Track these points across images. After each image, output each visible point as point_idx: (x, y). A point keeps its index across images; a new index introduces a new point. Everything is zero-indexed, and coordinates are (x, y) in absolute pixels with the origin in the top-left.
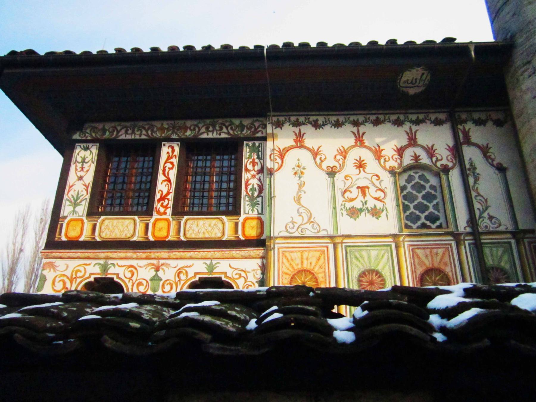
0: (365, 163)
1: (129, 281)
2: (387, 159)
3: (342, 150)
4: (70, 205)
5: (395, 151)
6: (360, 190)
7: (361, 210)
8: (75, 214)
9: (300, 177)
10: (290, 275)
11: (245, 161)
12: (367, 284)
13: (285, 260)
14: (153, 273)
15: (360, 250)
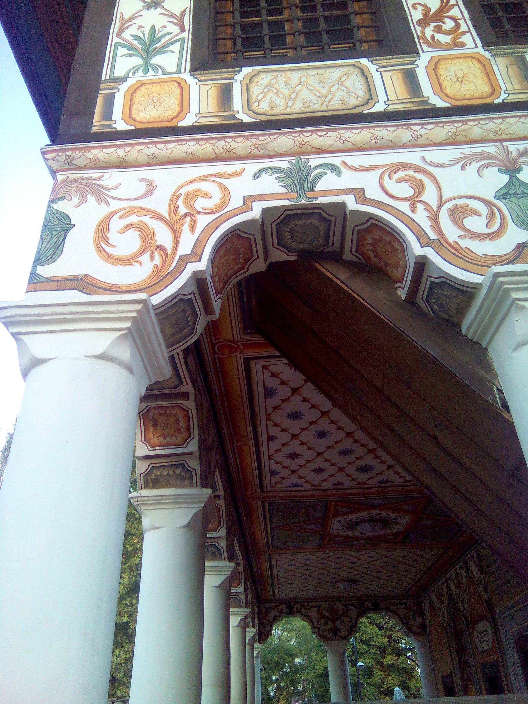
1: (413, 208)
4: (131, 55)
8: (151, 72)
14: (497, 179)
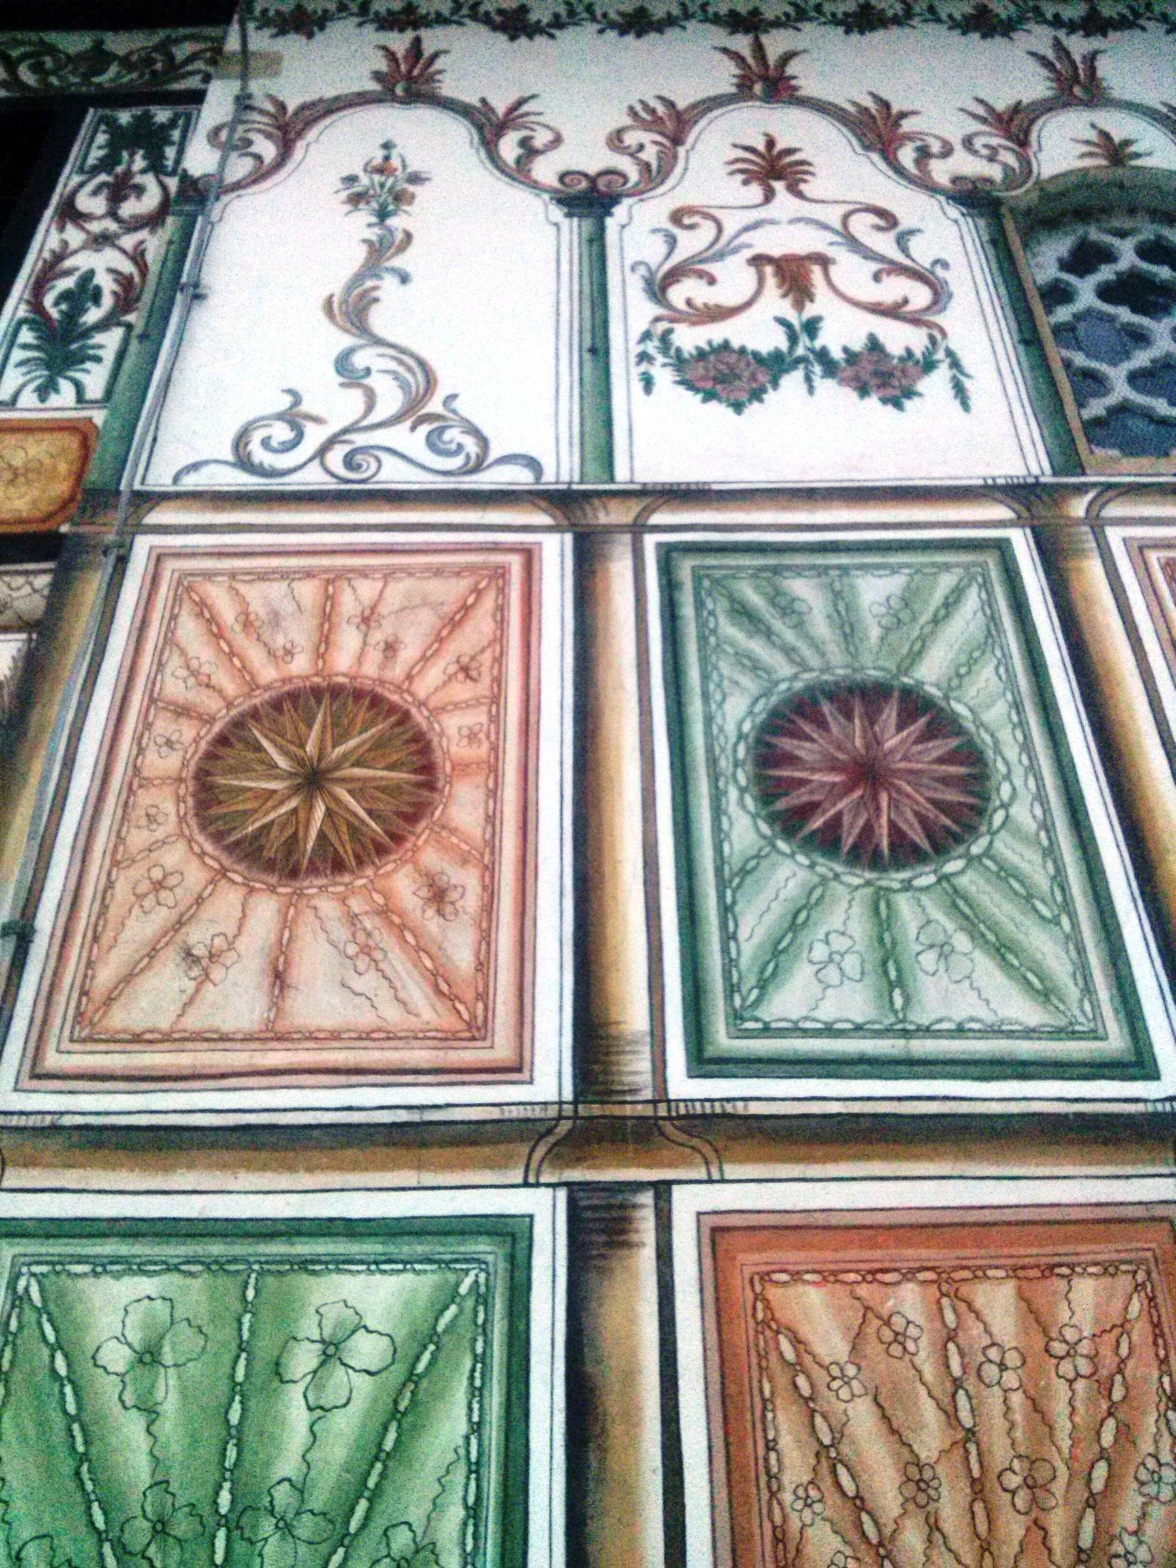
0: (803, 163)
2: (936, 147)
3: (661, 110)
5: (984, 120)
6: (769, 270)
7: (776, 365)
9: (383, 215)
10: (212, 720)
11: (68, 179)
12: (836, 778)
13: (189, 630)
15: (776, 570)
